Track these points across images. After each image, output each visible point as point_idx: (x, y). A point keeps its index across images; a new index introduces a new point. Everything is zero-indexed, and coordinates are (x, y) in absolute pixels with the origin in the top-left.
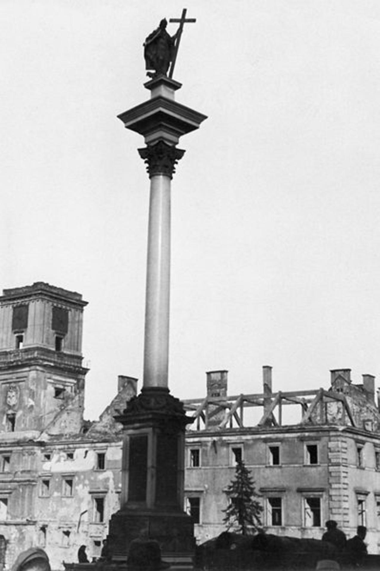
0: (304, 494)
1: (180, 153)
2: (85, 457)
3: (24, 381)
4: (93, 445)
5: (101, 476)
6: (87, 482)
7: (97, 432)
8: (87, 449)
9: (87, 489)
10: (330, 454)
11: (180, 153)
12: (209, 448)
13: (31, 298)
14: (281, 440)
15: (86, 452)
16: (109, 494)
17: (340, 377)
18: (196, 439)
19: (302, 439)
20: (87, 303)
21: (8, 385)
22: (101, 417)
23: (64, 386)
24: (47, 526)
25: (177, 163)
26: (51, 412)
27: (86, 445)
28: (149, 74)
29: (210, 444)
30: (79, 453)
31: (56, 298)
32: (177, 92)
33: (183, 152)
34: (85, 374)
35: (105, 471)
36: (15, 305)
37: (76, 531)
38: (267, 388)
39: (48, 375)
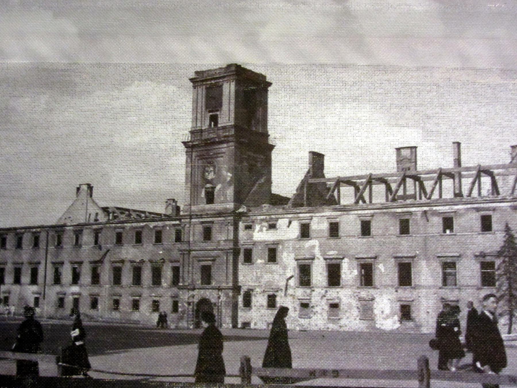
2: (288, 227)
3: (222, 157)
9: (292, 256)
13: (225, 79)
14: (494, 209)
16: (316, 261)
18: (405, 210)
24: (252, 290)
29: (419, 214)
30: (282, 223)
37: (283, 295)
38: (458, 162)
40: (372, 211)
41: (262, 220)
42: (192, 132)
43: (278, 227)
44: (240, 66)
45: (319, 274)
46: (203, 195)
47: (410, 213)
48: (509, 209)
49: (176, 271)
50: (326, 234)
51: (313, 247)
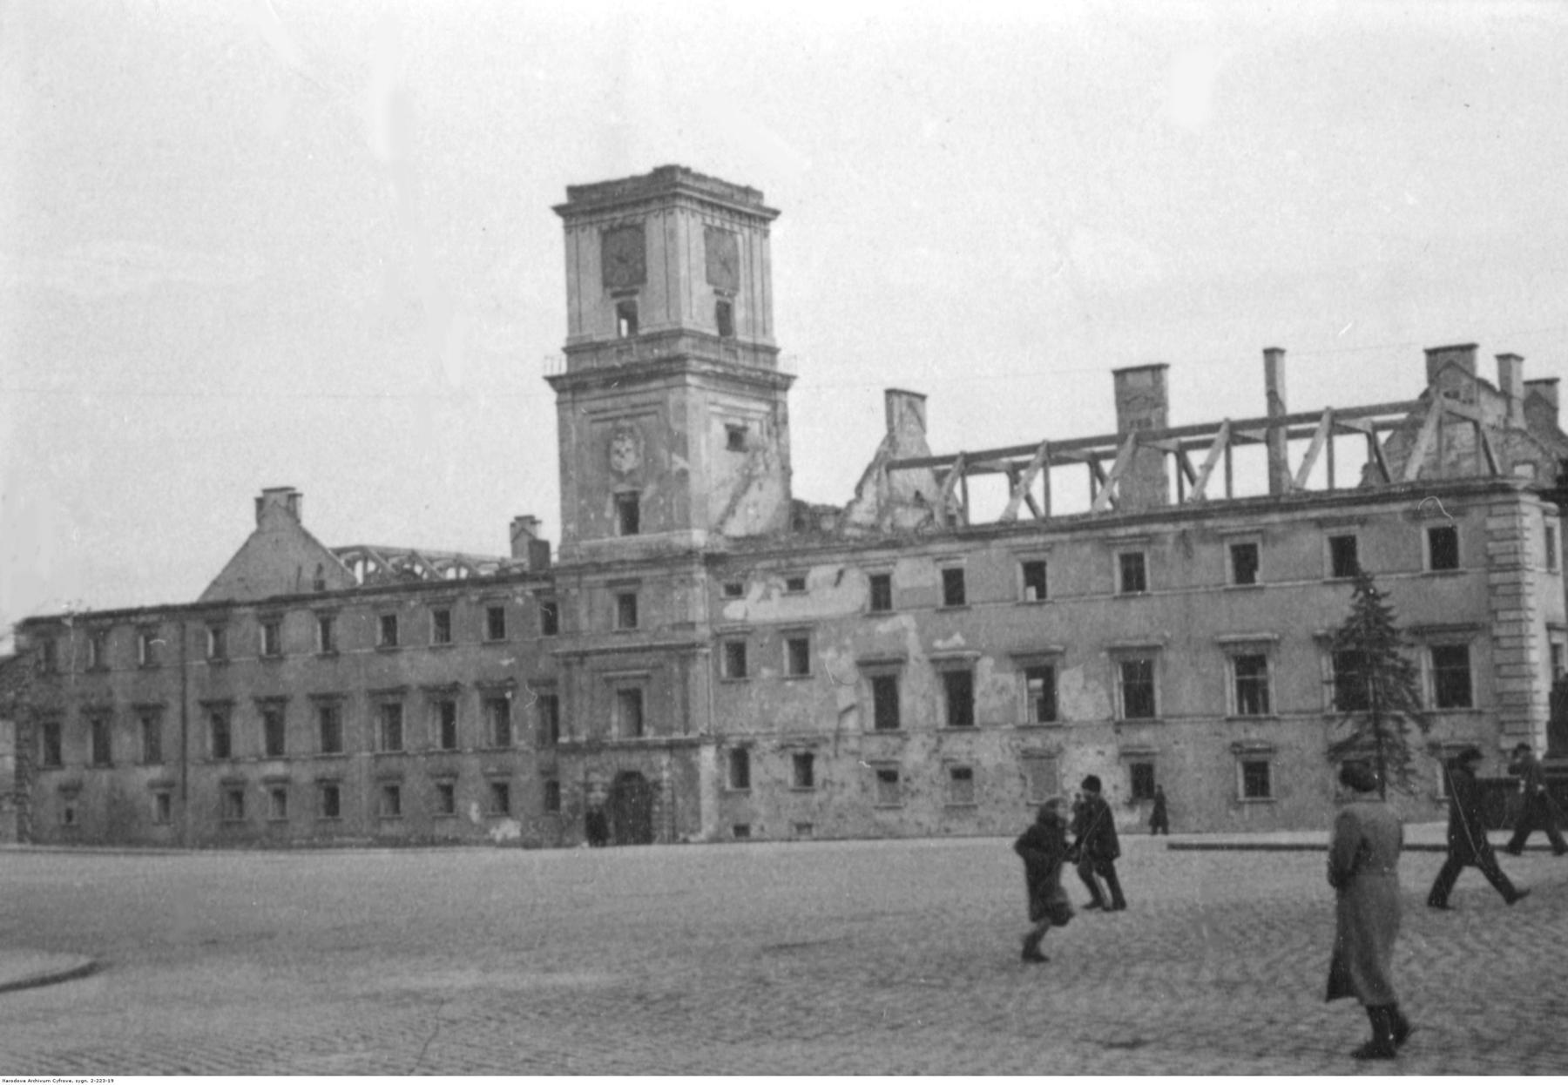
0: (1428, 638)
3: (655, 413)
4: (857, 556)
5: (884, 627)
6: (848, 641)
7: (857, 525)
8: (841, 566)
10: (1490, 545)
12: (1169, 548)
14: (1363, 521)
15: (841, 574)
17: (1450, 364)
18: (1135, 530)
19: (1416, 516)
21: (610, 425)
22: (859, 489)
23: (744, 419)
26: (723, 484)
27: (839, 557)
29: (1170, 539)
30: (819, 574)
31: (711, 205)
34: (786, 388)
35: (893, 615)
36: (605, 227)
37: (831, 754)
39: (711, 396)
40: (1051, 538)
41: (771, 570)
42: (571, 351)
43: (809, 584)
45: (921, 698)
46: (610, 511)
48: (1400, 518)
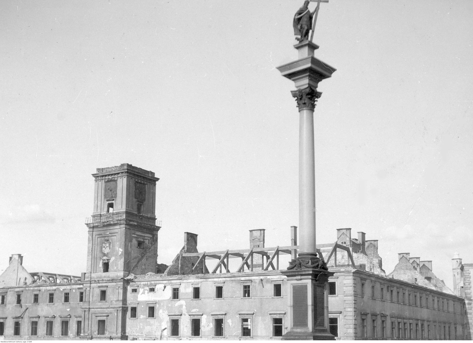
1: (318, 95)
9: (166, 312)
10: (344, 288)
11: (318, 95)
12: (257, 285)
13: (119, 175)
16: (183, 316)
18: (247, 278)
20: (158, 179)
21: (103, 239)
23: (144, 239)
25: (317, 101)
26: (135, 258)
28: (297, 39)
29: (258, 281)
30: (159, 287)
31: (138, 176)
32: (316, 51)
33: (320, 94)
34: (158, 230)
36: (106, 180)
39: (133, 232)
40: (224, 279)
41: (145, 285)
42: (94, 216)
43: (156, 290)
44: (131, 165)
46: (101, 265)
47: (251, 281)
49: (79, 323)
50: (191, 295)
51: (181, 306)
